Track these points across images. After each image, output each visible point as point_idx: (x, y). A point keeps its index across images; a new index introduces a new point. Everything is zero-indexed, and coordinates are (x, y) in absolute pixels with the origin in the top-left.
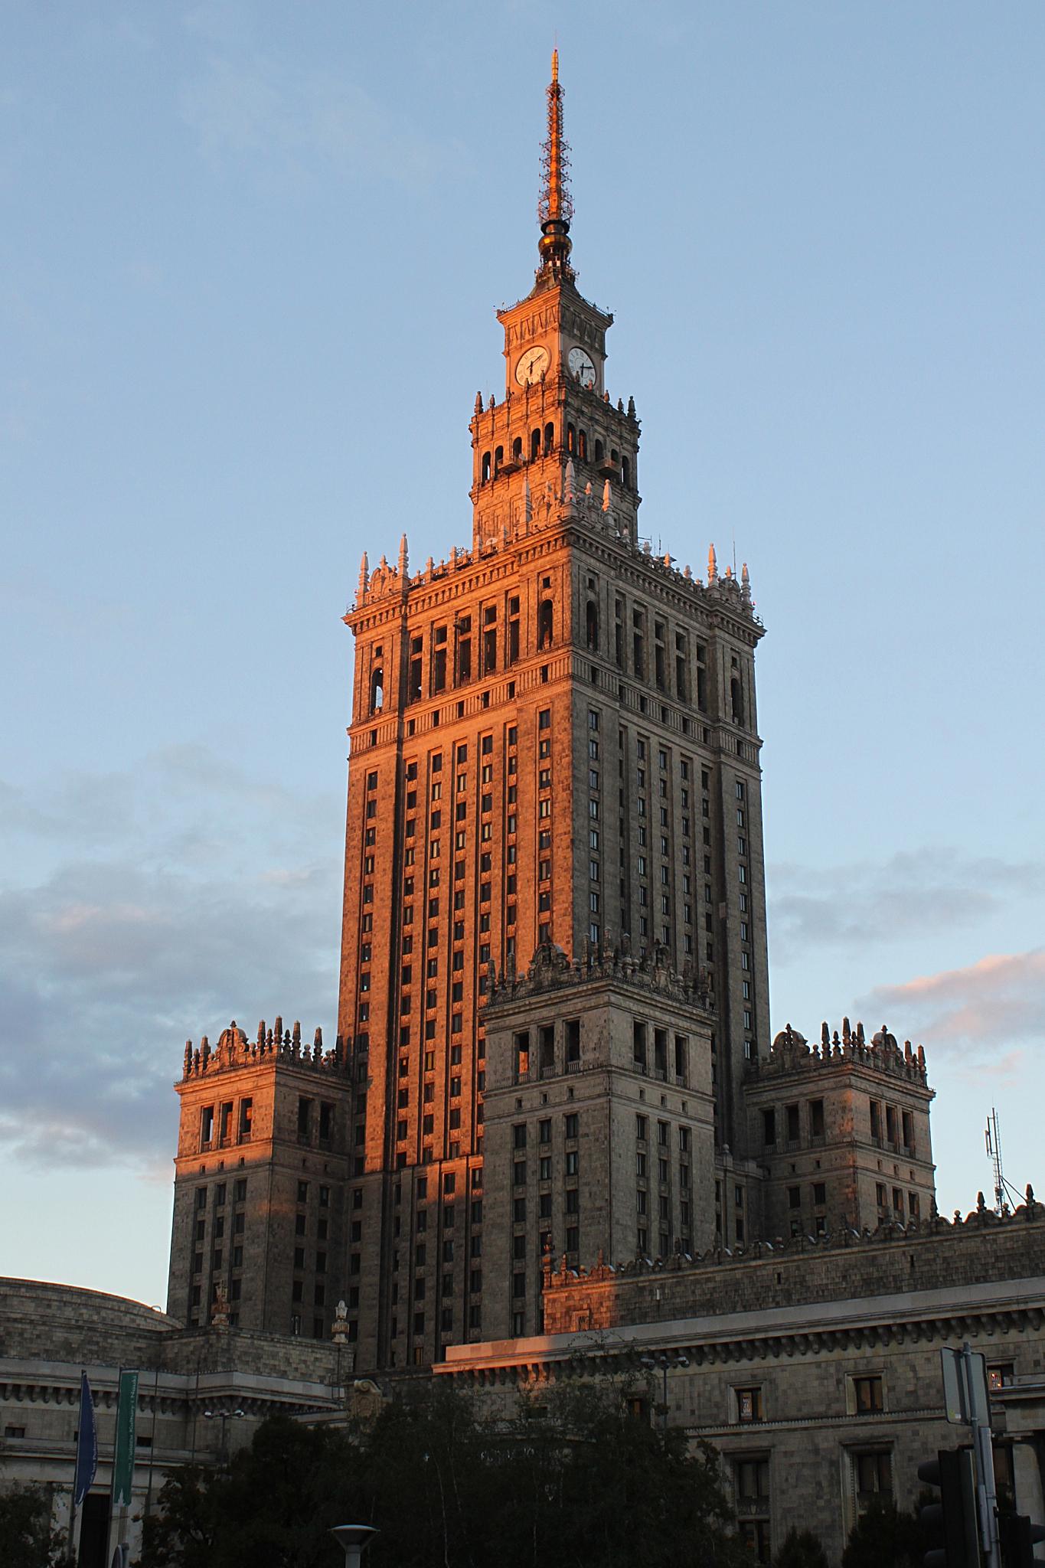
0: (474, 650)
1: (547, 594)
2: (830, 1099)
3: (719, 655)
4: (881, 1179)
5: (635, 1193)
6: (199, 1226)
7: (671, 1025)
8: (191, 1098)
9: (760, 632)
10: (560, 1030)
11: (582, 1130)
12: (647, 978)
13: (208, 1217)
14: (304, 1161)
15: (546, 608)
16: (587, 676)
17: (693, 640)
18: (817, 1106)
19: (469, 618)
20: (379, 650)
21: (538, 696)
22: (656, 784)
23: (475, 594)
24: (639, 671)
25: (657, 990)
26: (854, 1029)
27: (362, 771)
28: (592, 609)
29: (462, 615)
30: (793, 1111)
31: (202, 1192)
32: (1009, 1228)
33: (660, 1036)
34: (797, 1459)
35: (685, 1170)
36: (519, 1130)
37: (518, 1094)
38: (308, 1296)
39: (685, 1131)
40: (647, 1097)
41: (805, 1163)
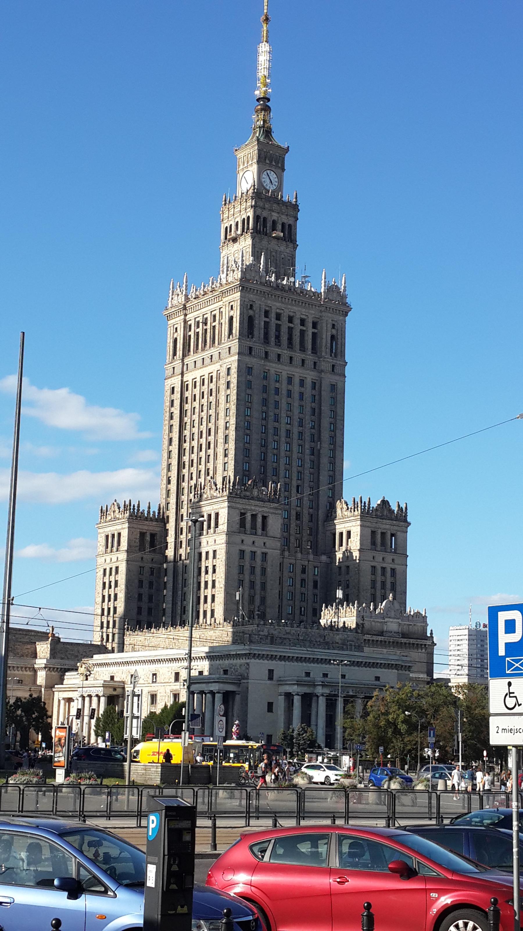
1: (232, 313)
3: (324, 325)
4: (373, 564)
11: (218, 556)
12: (248, 494)
14: (142, 558)
20: (176, 328)
21: (226, 361)
25: (253, 498)
27: (169, 385)
28: (251, 319)
29: (205, 316)
31: (105, 570)
33: (254, 517)
34: (162, 695)
35: (264, 571)
38: (145, 613)
39: (265, 554)
40: (244, 542)
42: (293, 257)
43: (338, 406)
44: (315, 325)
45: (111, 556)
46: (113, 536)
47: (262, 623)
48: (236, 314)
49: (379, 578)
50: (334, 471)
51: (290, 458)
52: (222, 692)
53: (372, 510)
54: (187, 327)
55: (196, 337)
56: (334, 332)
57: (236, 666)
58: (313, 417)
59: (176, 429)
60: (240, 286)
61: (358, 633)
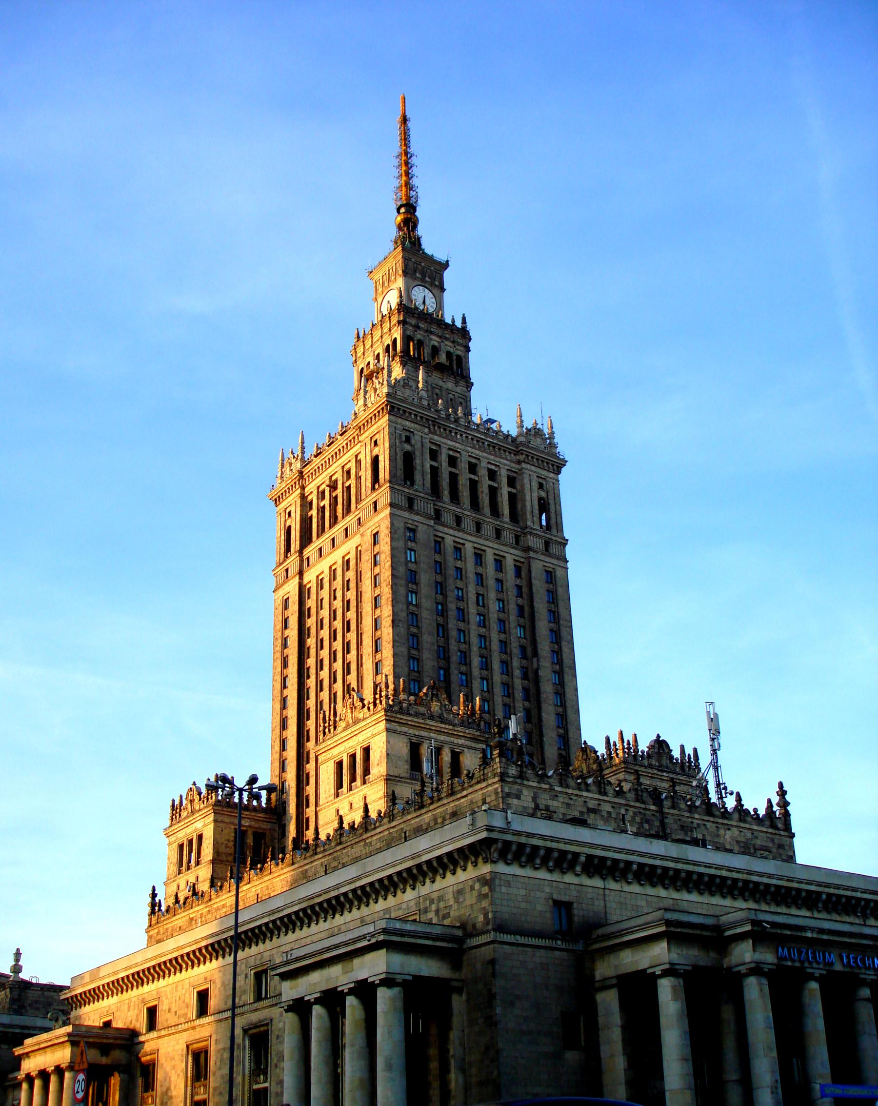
0: (340, 500)
1: (376, 451)
3: (526, 481)
8: (173, 839)
9: (564, 463)
12: (422, 709)
15: (375, 461)
16: (404, 503)
17: (503, 474)
19: (336, 481)
21: (371, 523)
22: (471, 576)
24: (455, 497)
25: (432, 717)
26: (628, 737)
27: (281, 598)
28: (408, 458)
29: (334, 478)
32: (378, 830)
37: (336, 806)
43: (561, 604)
44: (512, 482)
45: (186, 877)
46: (191, 842)
47: (513, 771)
48: (383, 452)
50: (563, 705)
51: (488, 679)
52: (399, 979)
53: (641, 756)
54: (305, 504)
55: (320, 514)
57: (441, 898)
58: (522, 620)
59: (293, 660)
60: (387, 405)
61: (778, 829)
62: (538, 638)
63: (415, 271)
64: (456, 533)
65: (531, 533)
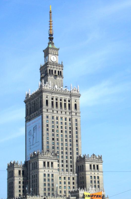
2: (84, 164)
3: (72, 101)
5: (43, 184)
6: (9, 187)
7: (50, 161)
10: (35, 163)
13: (10, 186)
16: (46, 111)
18: (83, 166)
23: (36, 98)
25: (47, 157)
30: (81, 166)
31: (9, 183)
35: (53, 180)
36: (33, 176)
41: (82, 174)
42: (62, 81)
44: (69, 101)
49: (93, 180)
56: (76, 103)
62: (73, 134)
63: (51, 52)
64: (57, 115)
65: (73, 112)
